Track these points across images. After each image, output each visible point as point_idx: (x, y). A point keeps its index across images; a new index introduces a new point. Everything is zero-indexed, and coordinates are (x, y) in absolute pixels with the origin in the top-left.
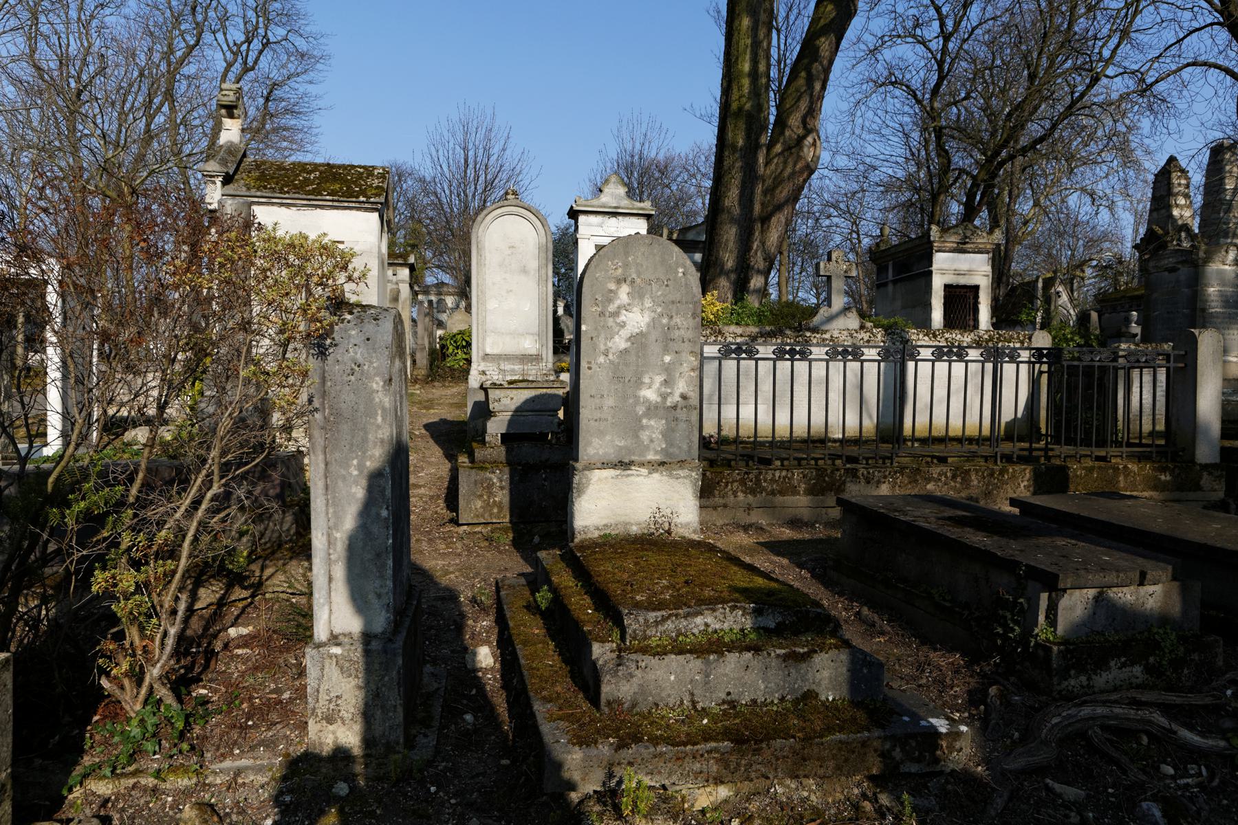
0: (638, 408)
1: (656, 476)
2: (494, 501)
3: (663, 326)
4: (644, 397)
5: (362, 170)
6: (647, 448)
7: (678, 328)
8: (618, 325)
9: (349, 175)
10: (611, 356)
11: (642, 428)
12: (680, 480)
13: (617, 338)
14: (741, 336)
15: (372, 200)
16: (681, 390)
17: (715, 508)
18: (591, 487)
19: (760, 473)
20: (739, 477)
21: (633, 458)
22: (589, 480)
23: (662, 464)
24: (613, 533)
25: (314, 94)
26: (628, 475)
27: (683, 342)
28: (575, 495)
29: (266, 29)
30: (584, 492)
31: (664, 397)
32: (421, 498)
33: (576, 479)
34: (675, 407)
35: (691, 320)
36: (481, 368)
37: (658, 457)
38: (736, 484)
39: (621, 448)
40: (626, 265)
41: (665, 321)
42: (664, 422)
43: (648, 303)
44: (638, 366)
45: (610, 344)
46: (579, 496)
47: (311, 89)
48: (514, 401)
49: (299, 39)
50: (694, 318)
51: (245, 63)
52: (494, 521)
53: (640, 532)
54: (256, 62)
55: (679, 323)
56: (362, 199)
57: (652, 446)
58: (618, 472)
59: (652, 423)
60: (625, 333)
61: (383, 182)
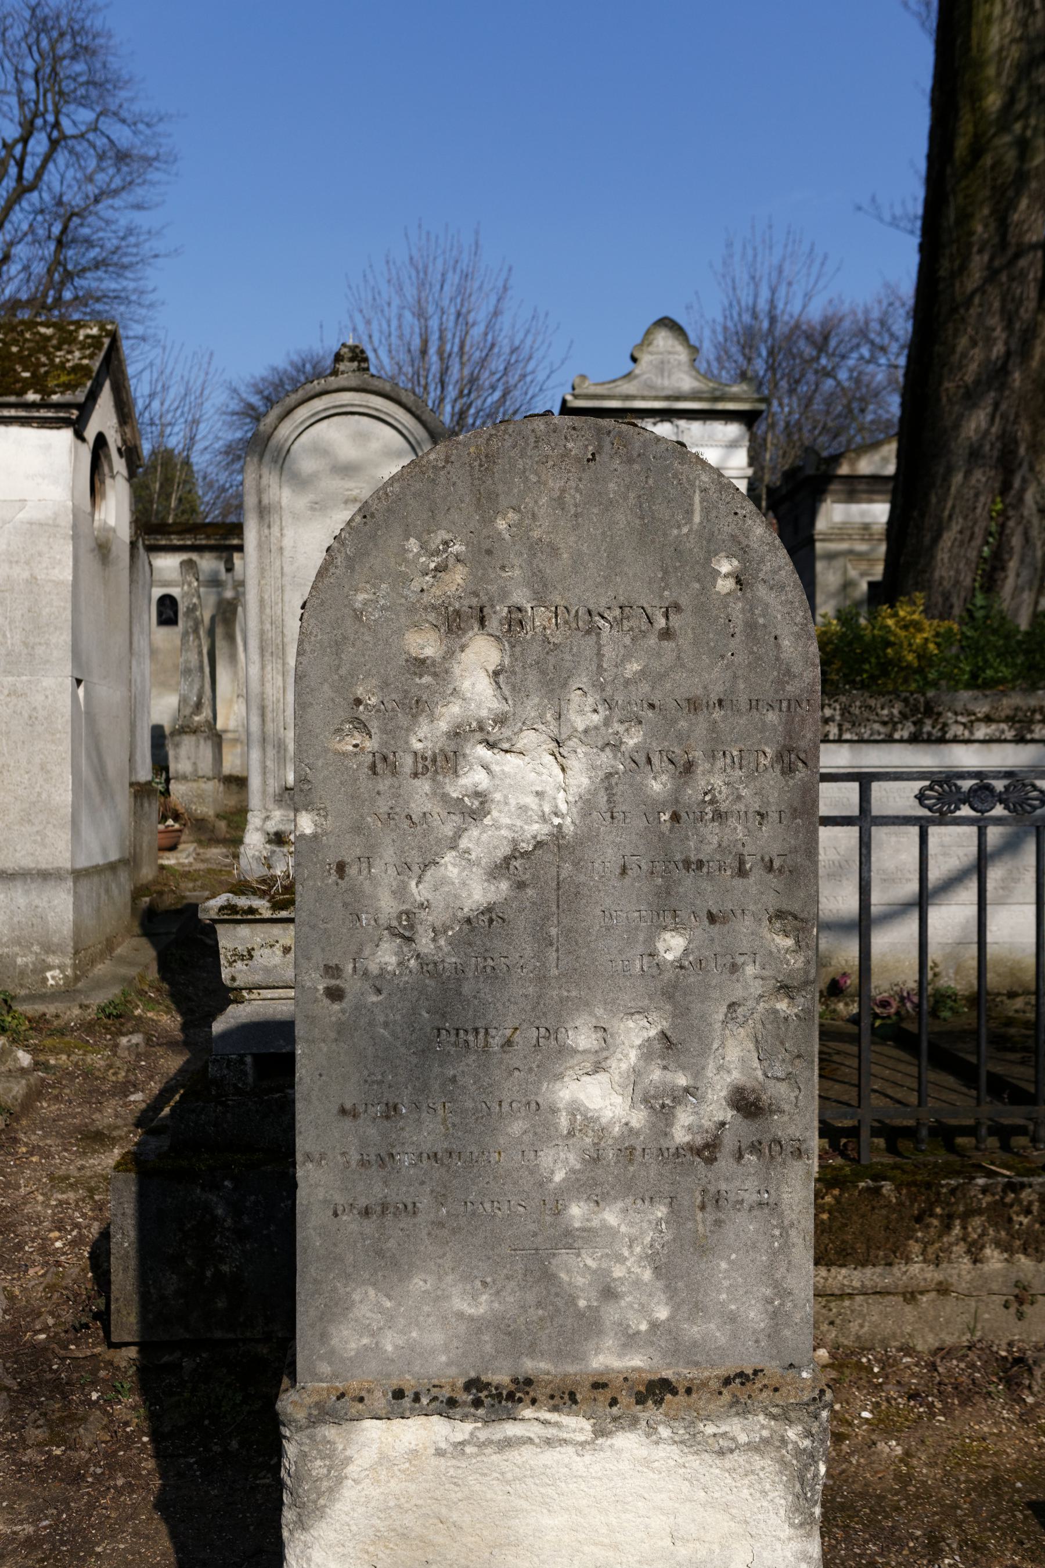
0: (546, 1158)
3: (652, 808)
4: (575, 1109)
5: (49, 331)
7: (720, 816)
8: (456, 807)
9: (15, 342)
10: (425, 943)
12: (730, 1461)
13: (450, 867)
14: (988, 719)
15: (55, 398)
16: (736, 1076)
17: (910, 1296)
18: (349, 1492)
20: (986, 1200)
21: (530, 1366)
22: (337, 1465)
25: (145, 228)
26: (508, 1443)
27: (742, 872)
28: (288, 1515)
29: (57, 113)
30: (320, 1512)
32: (91, 1191)
33: (291, 1449)
35: (773, 778)
36: (272, 827)
38: (977, 1221)
39: (477, 1326)
41: (658, 786)
42: (661, 1211)
44: (542, 979)
45: (419, 892)
46: (302, 1525)
47: (140, 219)
49: (119, 126)
50: (788, 770)
51: (20, 177)
52: (218, 1334)
54: (39, 175)
55: (723, 792)
56: (32, 397)
57: (611, 1314)
58: (463, 1430)
59: (611, 1217)
61: (91, 357)
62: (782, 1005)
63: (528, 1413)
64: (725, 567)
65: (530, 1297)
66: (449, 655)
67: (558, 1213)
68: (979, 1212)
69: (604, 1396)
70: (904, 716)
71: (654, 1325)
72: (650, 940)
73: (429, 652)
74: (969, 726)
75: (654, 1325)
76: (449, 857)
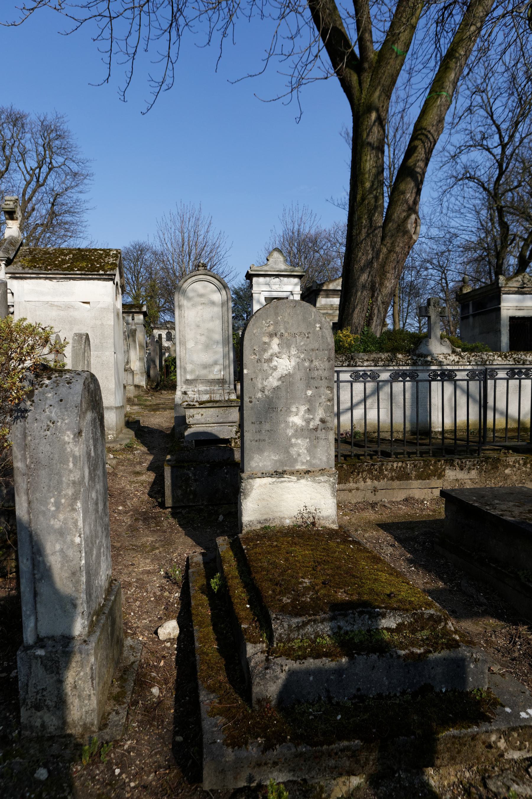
0: (288, 431)
1: (303, 481)
2: (191, 490)
3: (305, 368)
4: (293, 422)
5: (102, 252)
6: (296, 461)
7: (317, 370)
9: (92, 255)
11: (292, 445)
12: (321, 484)
13: (271, 379)
14: (367, 360)
15: (108, 273)
16: (321, 416)
17: (350, 491)
18: (254, 491)
19: (383, 465)
20: (367, 468)
22: (252, 486)
23: (308, 472)
24: (272, 525)
25: (83, 200)
26: (282, 482)
27: (321, 379)
28: (242, 497)
29: (51, 158)
30: (249, 495)
31: (308, 421)
32: (142, 484)
34: (316, 429)
35: (326, 363)
36: (183, 390)
37: (304, 467)
38: (365, 473)
39: (276, 461)
40: (276, 323)
41: (307, 364)
42: (308, 440)
43: (294, 351)
44: (287, 399)
45: (265, 383)
47: (82, 196)
48: (203, 416)
49: (73, 164)
50: (329, 361)
51: (38, 181)
52: (191, 504)
53: (292, 524)
54: (45, 181)
56: (101, 272)
57: (299, 459)
58: (274, 480)
59: (299, 441)
60: (277, 374)
61: (116, 260)
62: (329, 403)
63: (285, 476)
64: (318, 325)
65: (285, 456)
66: (270, 341)
67: (290, 441)
68: (365, 471)
69: (298, 473)
70: (346, 360)
71: (307, 461)
72: (306, 392)
73: (267, 341)
74: (362, 362)
75: (307, 461)
76: (270, 377)
